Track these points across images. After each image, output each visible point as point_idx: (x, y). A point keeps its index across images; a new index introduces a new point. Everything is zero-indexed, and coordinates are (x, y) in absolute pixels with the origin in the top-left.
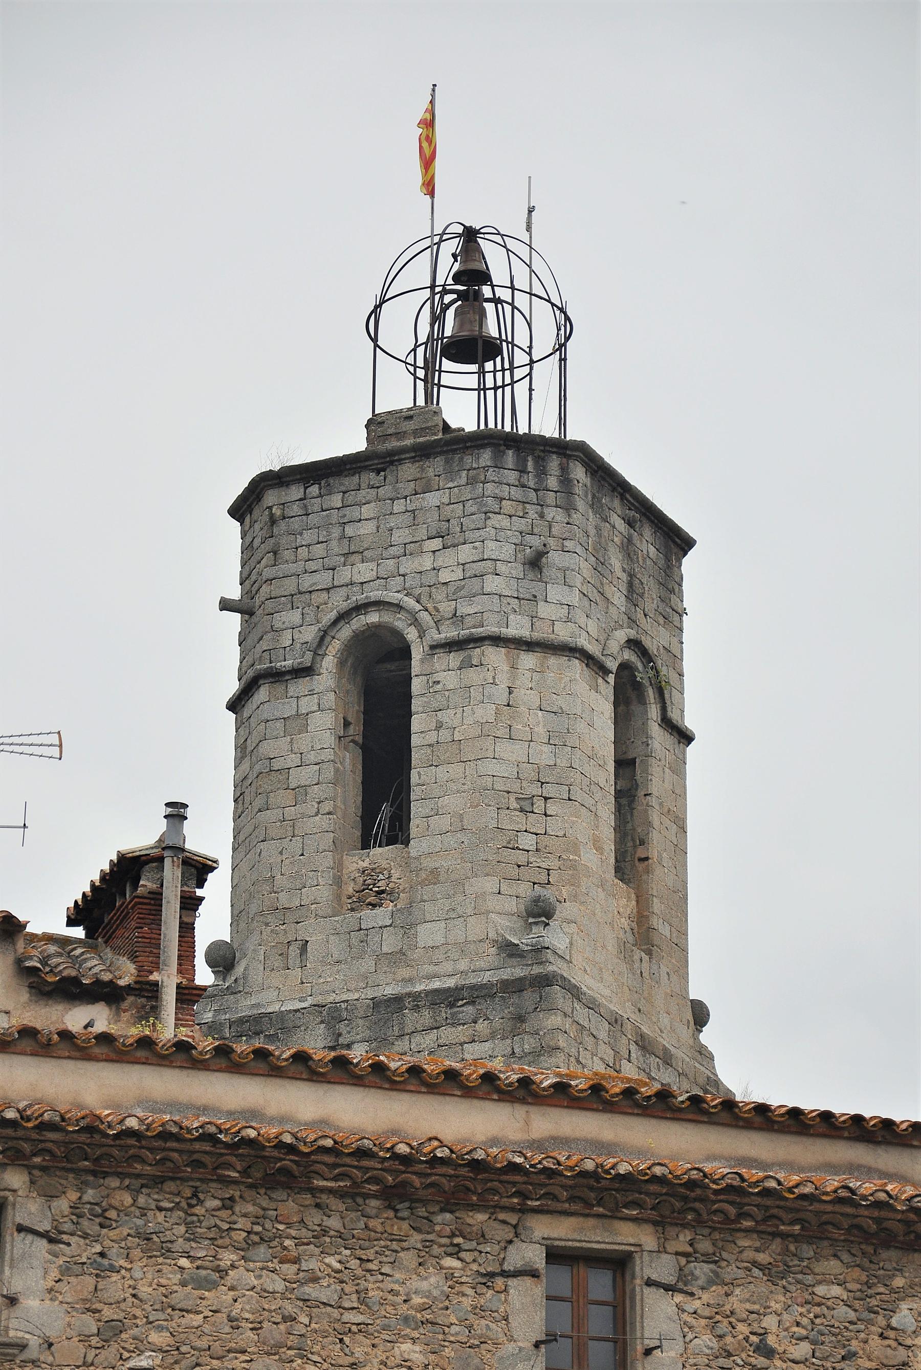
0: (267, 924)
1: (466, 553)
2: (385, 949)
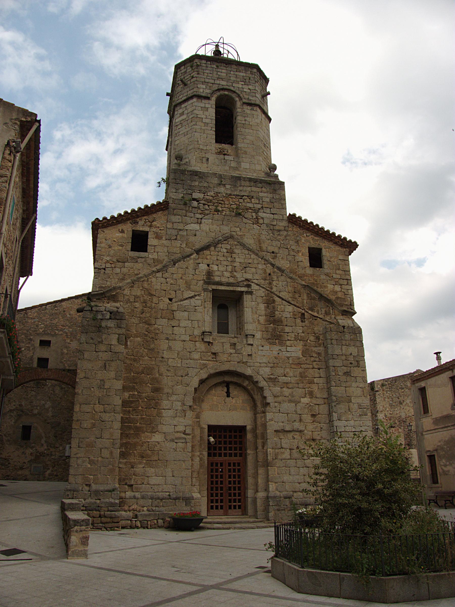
1: (250, 87)
2: (232, 165)
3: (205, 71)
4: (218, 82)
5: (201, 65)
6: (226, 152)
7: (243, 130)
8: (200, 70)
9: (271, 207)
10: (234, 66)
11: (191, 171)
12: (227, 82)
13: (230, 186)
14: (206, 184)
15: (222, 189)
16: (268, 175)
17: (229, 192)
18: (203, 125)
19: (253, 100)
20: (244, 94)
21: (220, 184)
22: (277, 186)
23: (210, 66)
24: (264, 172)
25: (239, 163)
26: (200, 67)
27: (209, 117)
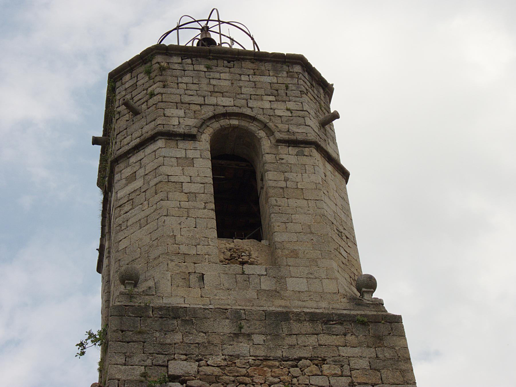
0: (172, 261)
1: (291, 105)
2: (263, 287)
3: (180, 80)
4: (213, 100)
5: (169, 68)
6: (246, 258)
7: (282, 202)
8: (169, 78)
9: (374, 381)
10: (248, 64)
11: (160, 308)
12: (235, 98)
13: (263, 337)
14: (201, 338)
15: (243, 347)
16: (357, 302)
17: (261, 352)
18: (184, 197)
19: (300, 132)
20: (278, 121)
21: (236, 335)
22: (383, 328)
23: (191, 67)
24: (345, 296)
25: (280, 280)
26: (169, 72)
27: (199, 179)
